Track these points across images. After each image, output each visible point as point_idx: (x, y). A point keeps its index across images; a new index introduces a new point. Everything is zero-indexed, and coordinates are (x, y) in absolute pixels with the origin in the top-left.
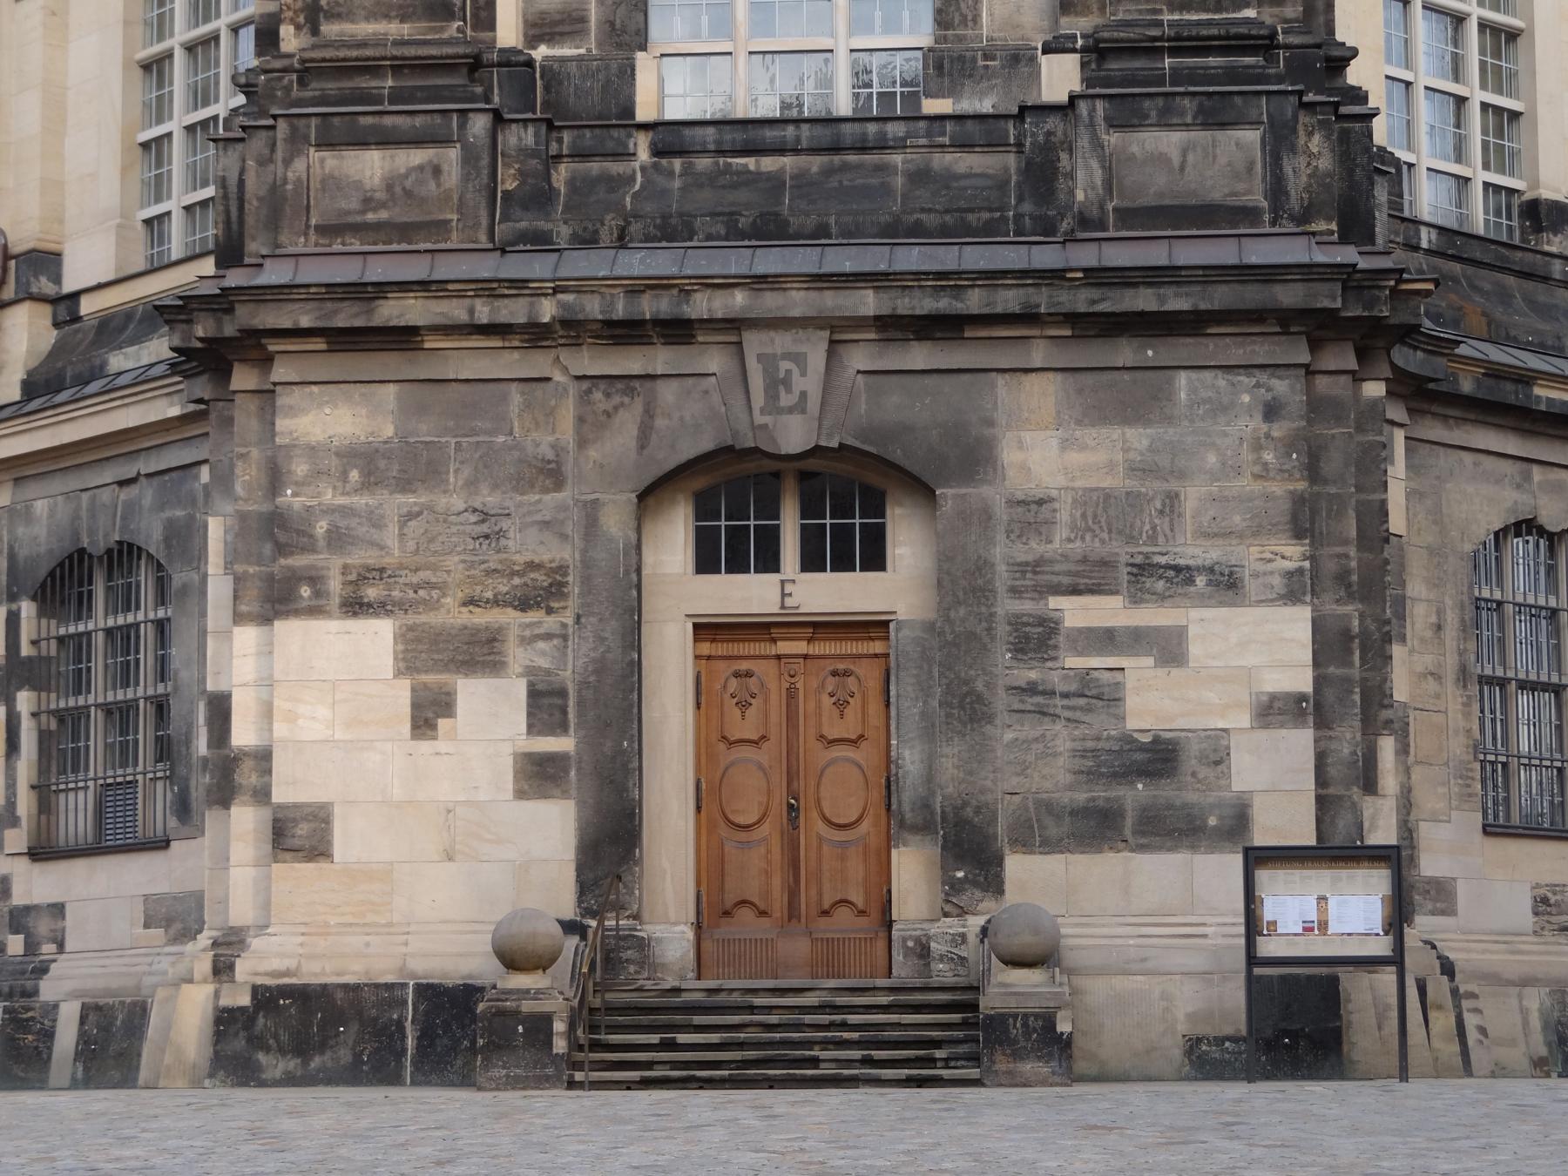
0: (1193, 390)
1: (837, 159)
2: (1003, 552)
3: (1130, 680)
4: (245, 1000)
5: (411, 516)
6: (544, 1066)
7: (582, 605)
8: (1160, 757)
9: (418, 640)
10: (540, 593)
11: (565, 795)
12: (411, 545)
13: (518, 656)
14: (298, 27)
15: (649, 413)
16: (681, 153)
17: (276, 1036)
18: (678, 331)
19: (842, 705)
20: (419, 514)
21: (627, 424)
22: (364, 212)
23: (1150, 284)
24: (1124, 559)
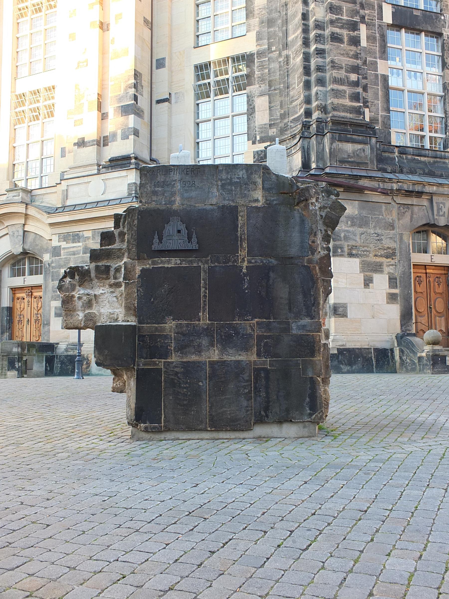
1: (435, 160)
4: (336, 352)
6: (445, 368)
7: (400, 258)
9: (364, 264)
10: (391, 255)
11: (397, 303)
12: (362, 241)
13: (386, 269)
14: (322, 112)
15: (412, 214)
16: (405, 154)
17: (344, 361)
18: (419, 194)
20: (364, 233)
21: (408, 214)
22: (348, 158)
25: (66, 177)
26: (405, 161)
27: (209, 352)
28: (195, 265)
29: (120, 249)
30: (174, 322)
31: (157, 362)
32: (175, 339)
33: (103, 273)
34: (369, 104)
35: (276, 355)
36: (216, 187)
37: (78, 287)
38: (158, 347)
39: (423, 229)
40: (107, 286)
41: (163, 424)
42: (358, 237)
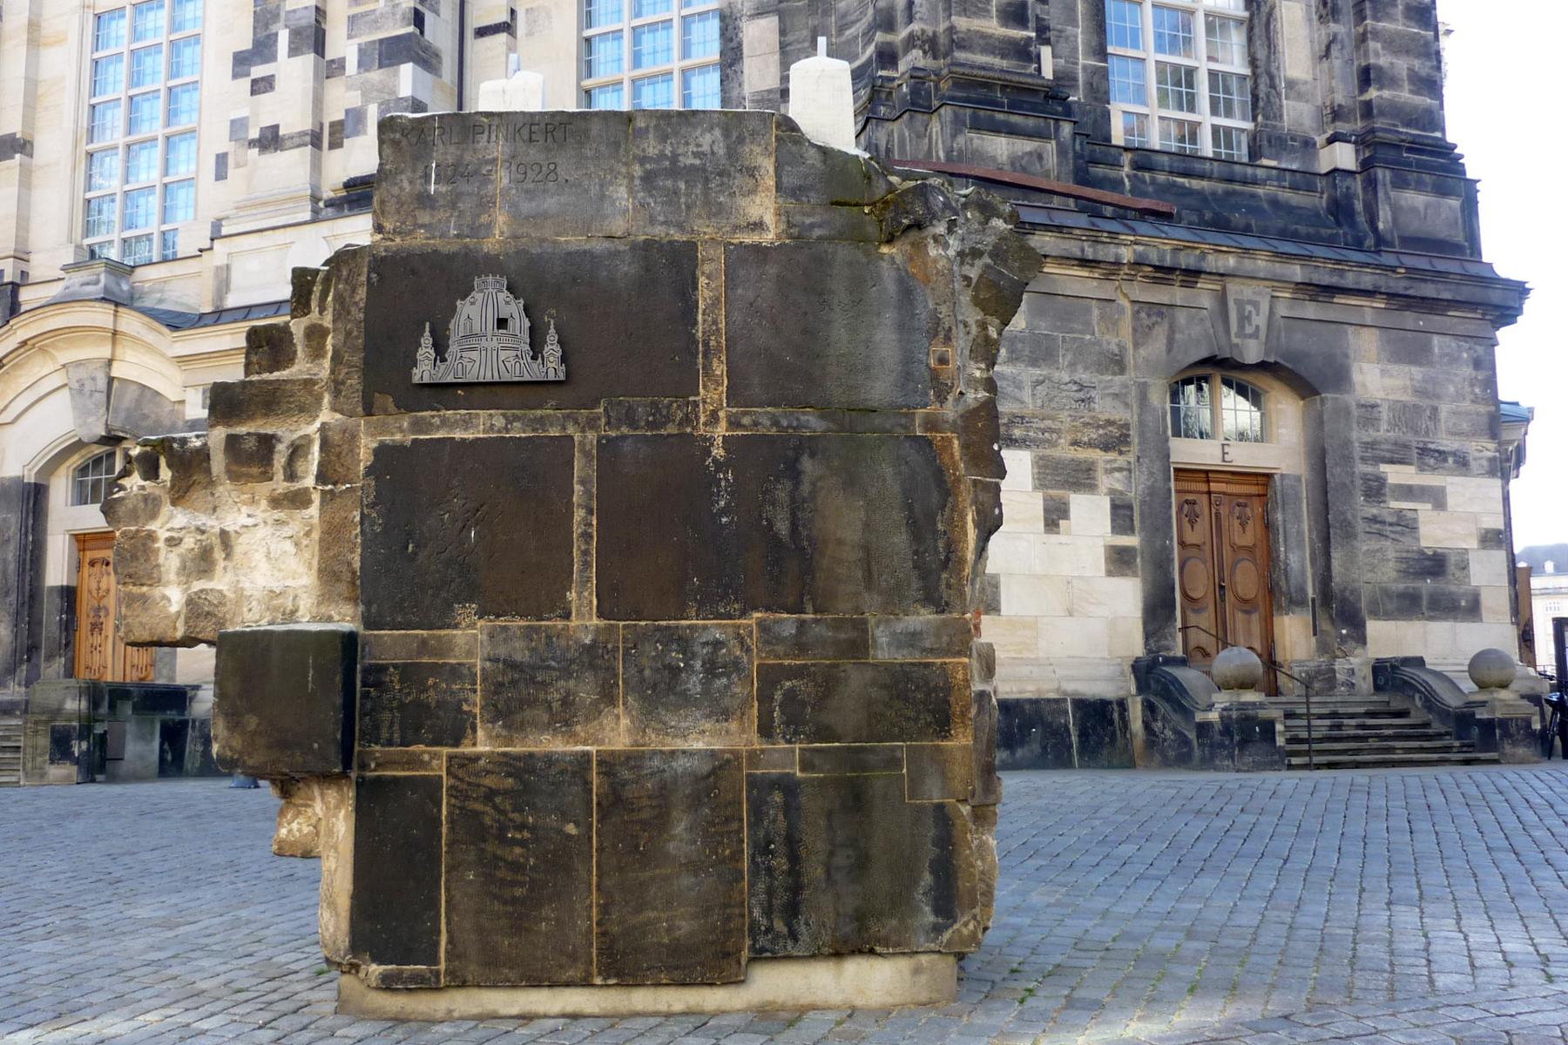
0: (1441, 348)
2: (1358, 435)
3: (1422, 517)
5: (1039, 383)
7: (1141, 450)
8: (1435, 564)
10: (1115, 442)
11: (1135, 575)
12: (1039, 402)
13: (1105, 481)
14: (925, 53)
16: (1150, 169)
18: (1192, 275)
19: (1243, 525)
21: (1161, 333)
23: (1433, 282)
24: (1414, 444)
25: (224, 231)
26: (1150, 189)
27: (601, 724)
28: (554, 432)
29: (309, 383)
30: (480, 623)
31: (426, 757)
32: (484, 680)
33: (253, 458)
34: (1052, 35)
35: (824, 733)
36: (625, 182)
37: (167, 508)
38: (428, 707)
39: (1200, 372)
40: (264, 503)
41: (443, 966)
42: (1027, 391)
